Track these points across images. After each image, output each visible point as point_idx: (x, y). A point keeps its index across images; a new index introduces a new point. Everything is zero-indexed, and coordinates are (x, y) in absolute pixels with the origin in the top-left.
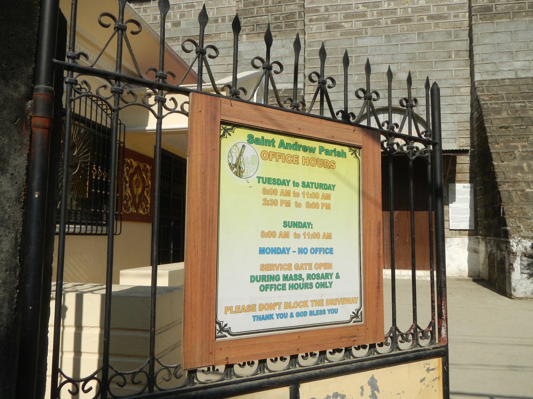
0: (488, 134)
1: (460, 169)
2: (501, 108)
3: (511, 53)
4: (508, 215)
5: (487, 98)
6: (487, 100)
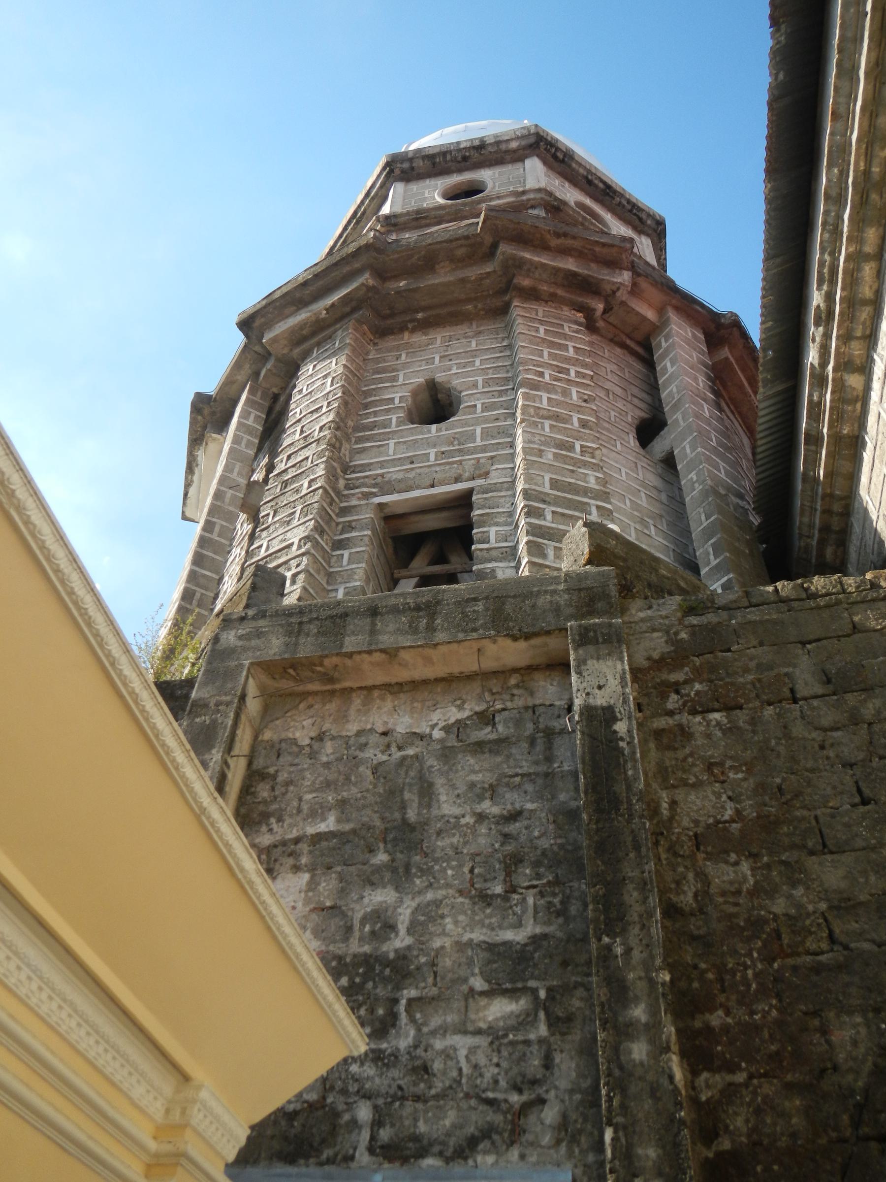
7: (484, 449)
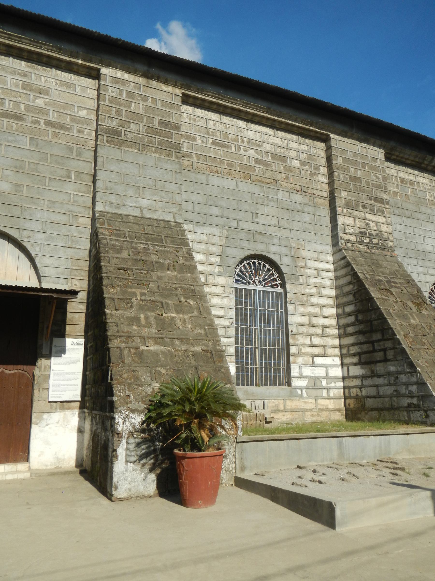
0: (103, 275)
1: (70, 320)
2: (122, 247)
3: (138, 187)
4: (117, 379)
5: (107, 233)
6: (107, 235)
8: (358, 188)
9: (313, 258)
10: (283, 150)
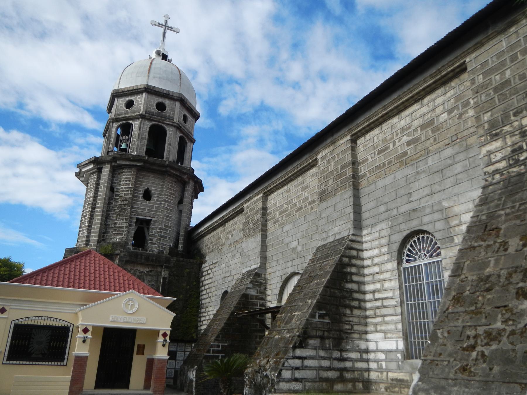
7: (155, 211)
8: (506, 95)
9: (468, 209)
10: (430, 115)
